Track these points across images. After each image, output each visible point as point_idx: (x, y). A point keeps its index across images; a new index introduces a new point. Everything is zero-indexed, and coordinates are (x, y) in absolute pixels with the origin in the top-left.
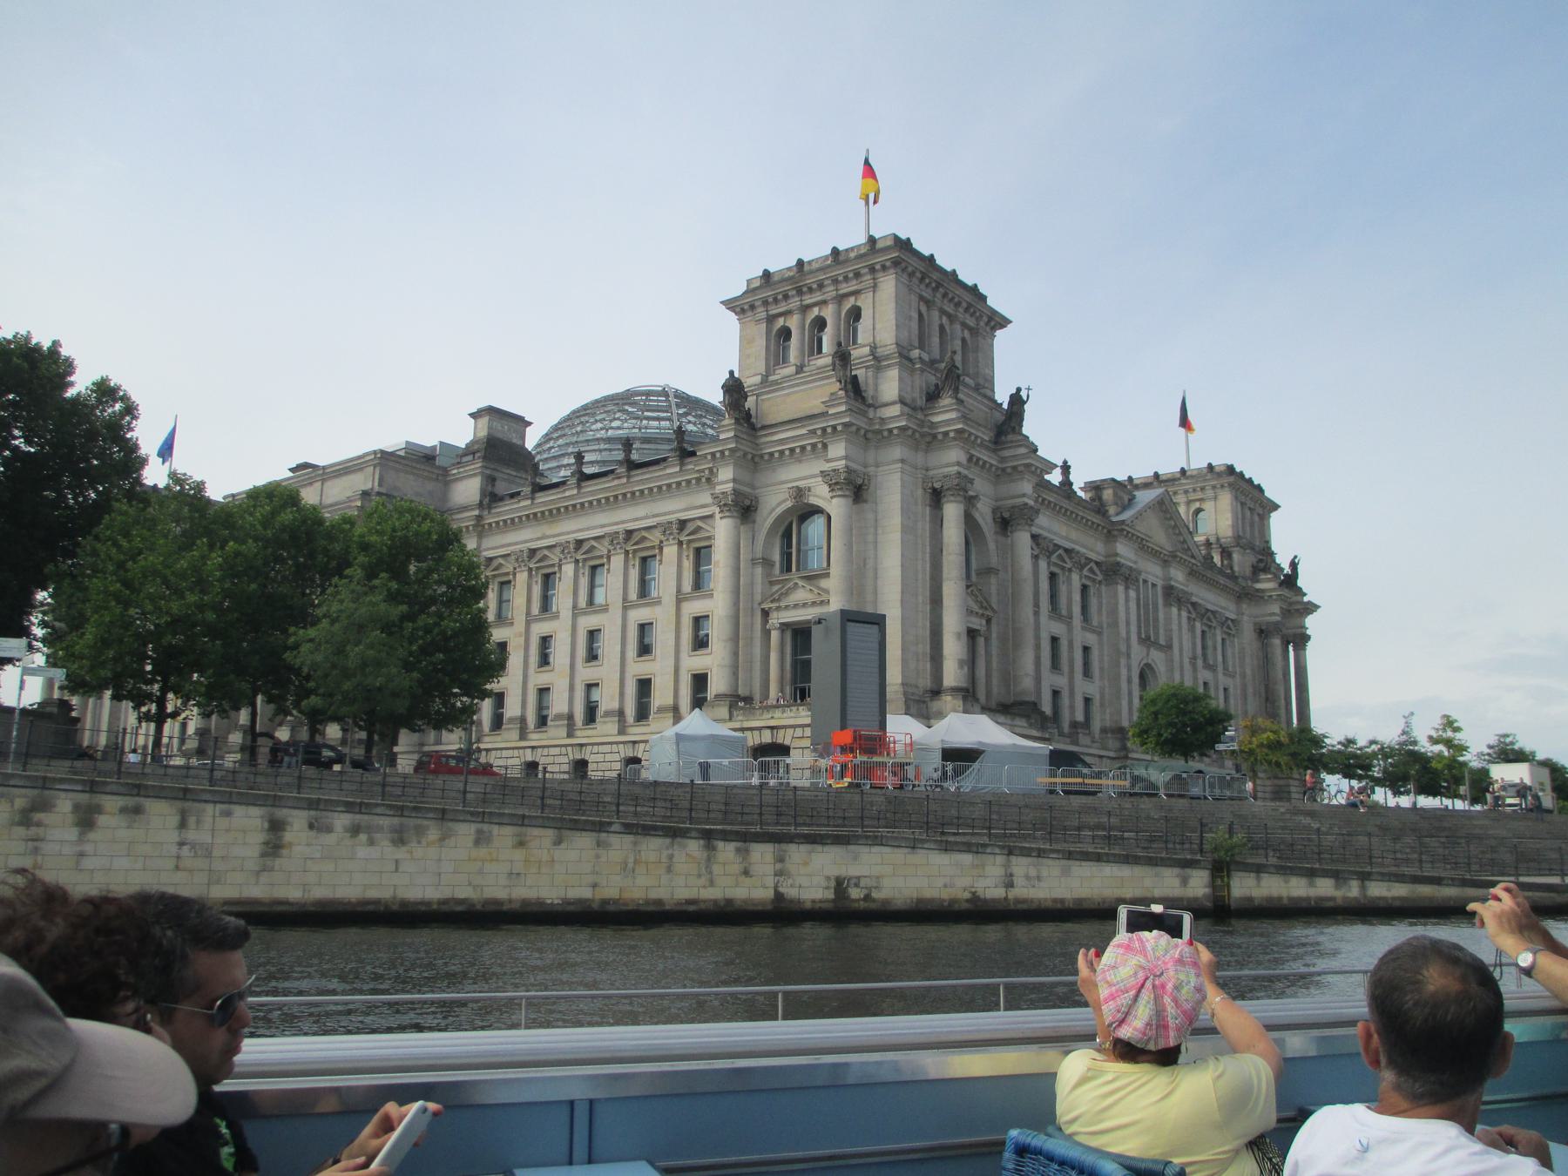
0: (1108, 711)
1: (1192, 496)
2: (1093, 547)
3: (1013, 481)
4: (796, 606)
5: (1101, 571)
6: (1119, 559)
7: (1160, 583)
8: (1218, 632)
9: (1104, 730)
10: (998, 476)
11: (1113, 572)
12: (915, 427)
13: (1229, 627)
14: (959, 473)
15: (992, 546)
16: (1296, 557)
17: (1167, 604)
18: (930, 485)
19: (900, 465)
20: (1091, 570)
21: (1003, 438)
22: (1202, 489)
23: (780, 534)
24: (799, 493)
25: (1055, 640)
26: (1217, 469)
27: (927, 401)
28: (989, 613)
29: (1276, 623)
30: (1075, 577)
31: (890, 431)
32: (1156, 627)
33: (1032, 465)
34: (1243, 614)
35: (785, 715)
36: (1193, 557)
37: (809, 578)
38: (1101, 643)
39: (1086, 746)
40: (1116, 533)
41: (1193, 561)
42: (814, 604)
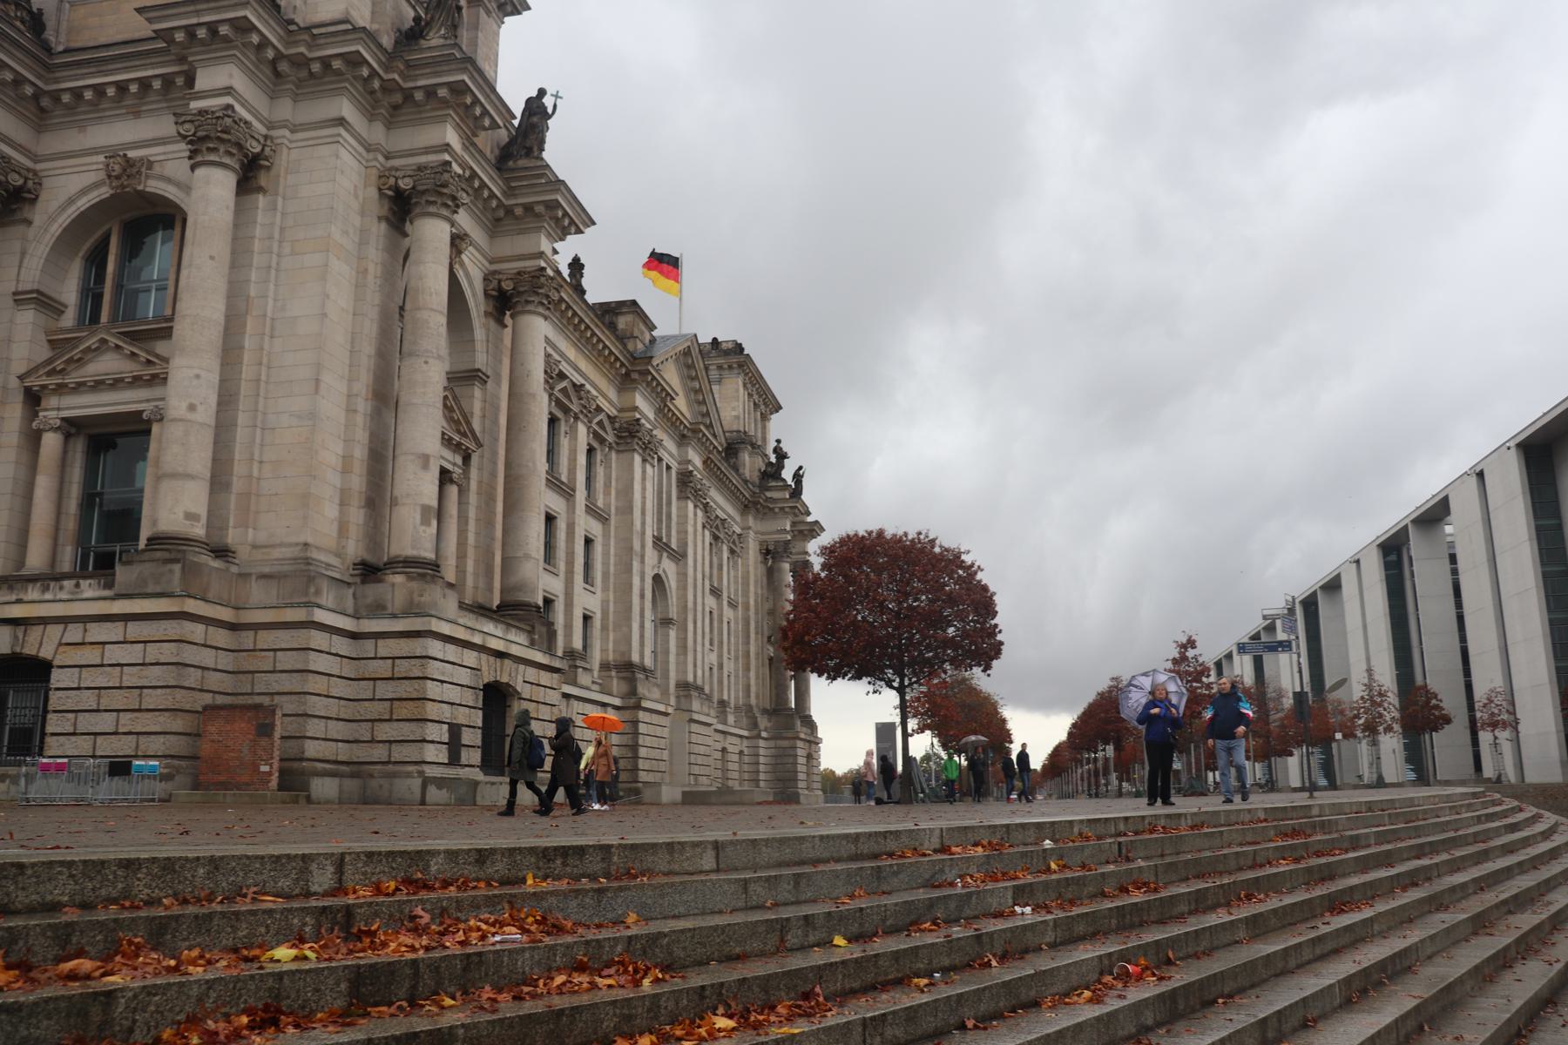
0: (611, 638)
2: (604, 392)
3: (522, 232)
4: (98, 385)
7: (674, 465)
8: (725, 548)
9: (605, 666)
10: (498, 220)
11: (628, 434)
13: (734, 543)
15: (479, 334)
16: (801, 468)
17: (682, 497)
18: (392, 181)
20: (600, 423)
21: (511, 163)
23: (81, 254)
24: (125, 169)
25: (550, 519)
26: (724, 346)
27: (397, 42)
29: (787, 543)
30: (582, 429)
31: (326, 62)
32: (669, 527)
34: (749, 528)
35: (48, 596)
36: (715, 436)
37: (133, 337)
38: (606, 535)
39: (587, 688)
40: (635, 376)
42: (137, 381)
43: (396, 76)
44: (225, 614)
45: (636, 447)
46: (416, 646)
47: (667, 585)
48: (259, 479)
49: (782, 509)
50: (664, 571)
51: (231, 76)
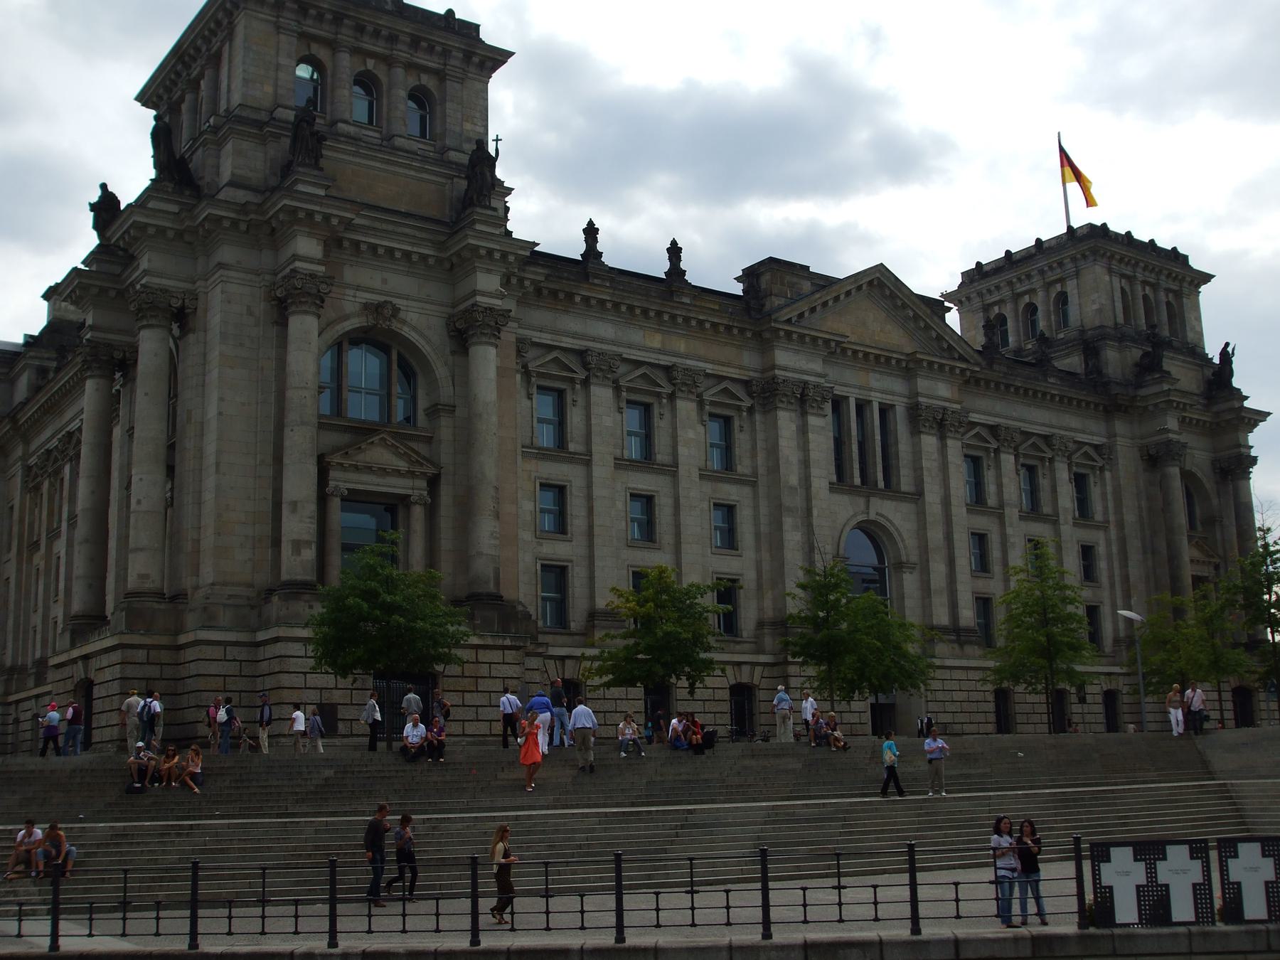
1: (1051, 276)
5: (750, 395)
6: (777, 372)
9: (760, 624)
12: (232, 215)
13: (1086, 455)
14: (294, 271)
15: (441, 371)
16: (1227, 345)
17: (915, 432)
19: (221, 272)
22: (1061, 264)
26: (1079, 233)
28: (431, 470)
31: (201, 224)
33: (478, 247)
34: (1115, 436)
38: (756, 496)
41: (964, 366)
43: (252, 216)
44: (164, 640)
45: (780, 405)
46: (279, 649)
47: (892, 529)
48: (199, 541)
49: (1156, 405)
50: (882, 516)
51: (149, 261)
